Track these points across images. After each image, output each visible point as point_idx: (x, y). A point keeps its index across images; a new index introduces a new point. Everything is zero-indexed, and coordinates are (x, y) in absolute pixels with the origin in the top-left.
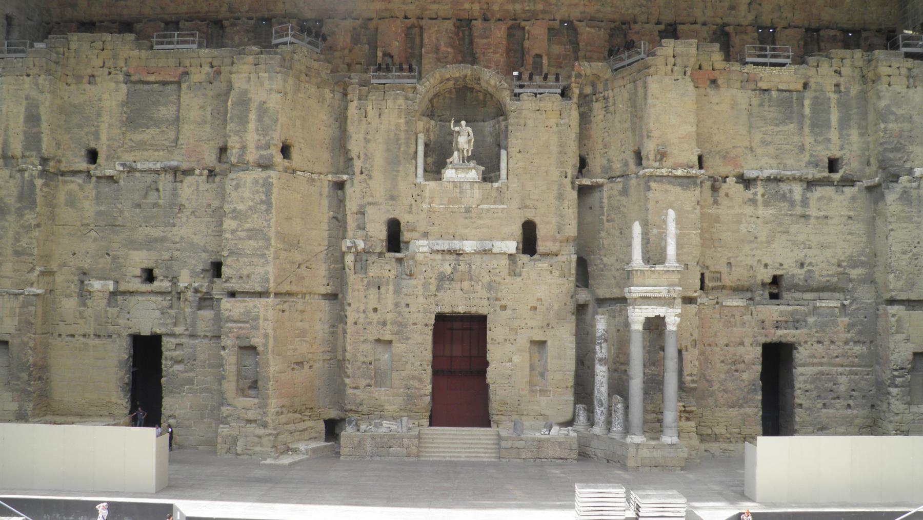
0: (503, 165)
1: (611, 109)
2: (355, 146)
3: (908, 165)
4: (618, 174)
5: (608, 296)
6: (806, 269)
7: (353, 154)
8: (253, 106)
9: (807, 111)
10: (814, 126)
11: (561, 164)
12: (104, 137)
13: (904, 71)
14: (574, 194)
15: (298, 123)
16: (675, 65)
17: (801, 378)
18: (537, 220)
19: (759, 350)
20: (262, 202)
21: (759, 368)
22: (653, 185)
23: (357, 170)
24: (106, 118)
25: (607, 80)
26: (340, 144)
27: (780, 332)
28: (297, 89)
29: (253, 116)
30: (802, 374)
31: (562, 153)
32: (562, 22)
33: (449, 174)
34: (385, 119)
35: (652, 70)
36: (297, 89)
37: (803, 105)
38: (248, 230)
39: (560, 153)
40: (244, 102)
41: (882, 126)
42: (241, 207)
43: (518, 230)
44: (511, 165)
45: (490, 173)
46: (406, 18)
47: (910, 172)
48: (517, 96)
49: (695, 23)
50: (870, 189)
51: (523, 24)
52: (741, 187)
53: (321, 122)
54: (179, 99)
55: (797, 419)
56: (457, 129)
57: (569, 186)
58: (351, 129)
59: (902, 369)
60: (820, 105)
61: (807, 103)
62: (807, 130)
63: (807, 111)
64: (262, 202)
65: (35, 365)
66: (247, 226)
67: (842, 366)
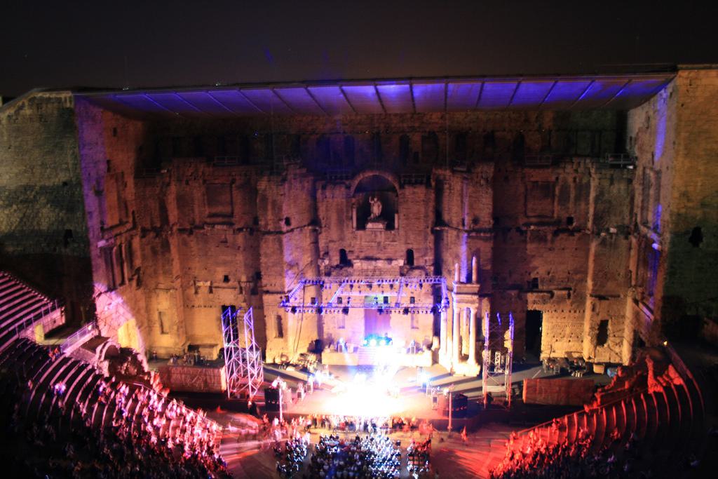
0: (396, 221)
1: (452, 191)
2: (322, 214)
3: (606, 226)
7: (321, 217)
8: (270, 200)
9: (557, 192)
10: (559, 201)
11: (426, 222)
12: (197, 211)
13: (608, 176)
14: (431, 238)
15: (292, 206)
20: (278, 249)
21: (524, 322)
23: (323, 225)
24: (196, 202)
26: (314, 209)
27: (535, 306)
28: (290, 189)
29: (270, 207)
31: (426, 216)
32: (429, 132)
33: (369, 225)
34: (334, 200)
36: (290, 189)
38: (272, 262)
39: (425, 217)
40: (264, 199)
42: (268, 252)
43: (404, 253)
44: (400, 222)
45: (390, 226)
46: (344, 132)
47: (608, 230)
49: (504, 130)
52: (518, 234)
53: (303, 198)
54: (231, 192)
56: (372, 202)
57: (430, 233)
58: (320, 205)
62: (556, 204)
64: (278, 249)
65: (179, 322)
66: (271, 261)
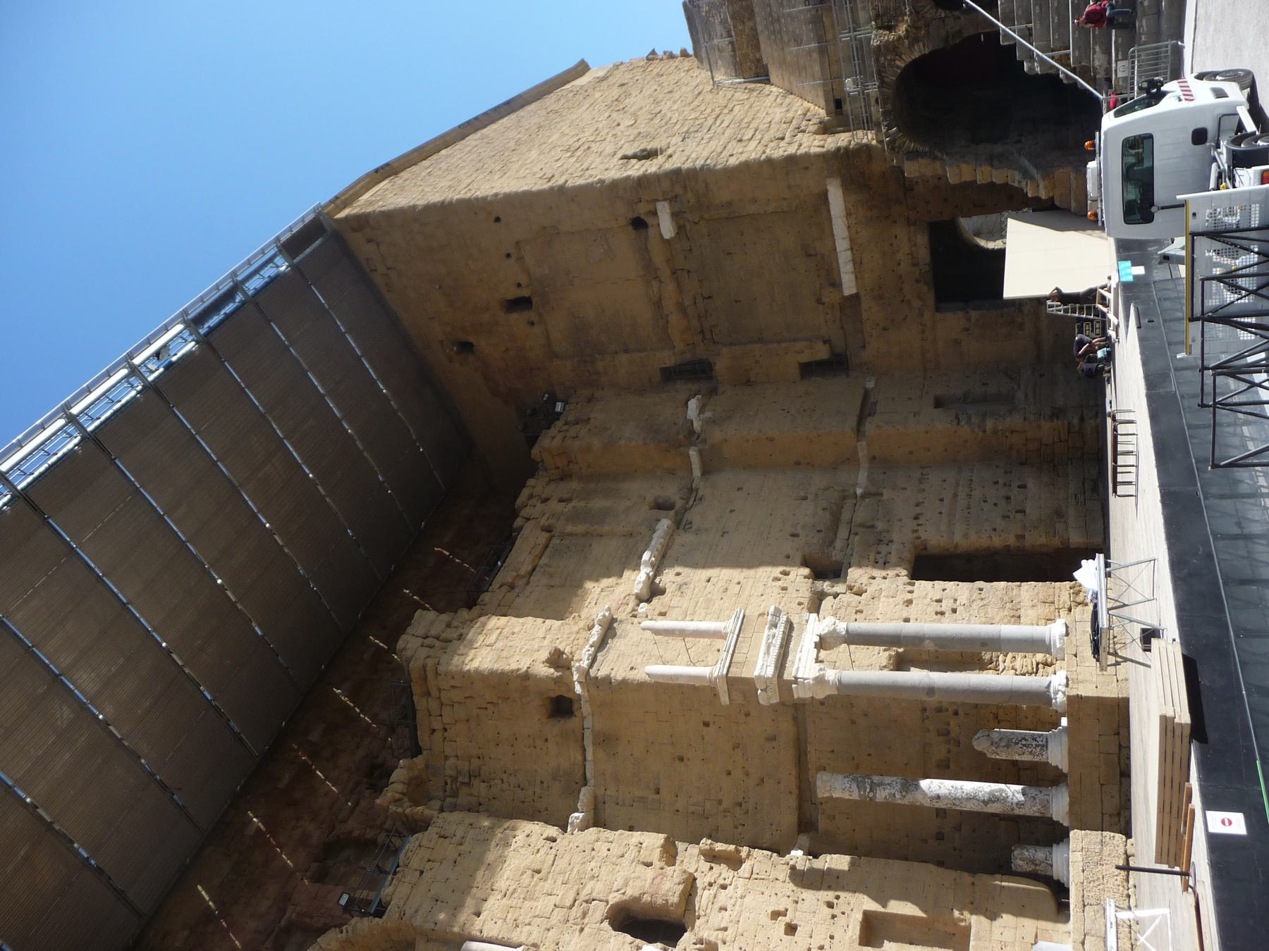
1: (475, 762)
4: (580, 758)
5: (793, 802)
6: (799, 531)
9: (580, 529)
16: (437, 638)
17: (973, 537)
18: (614, 898)
19: (917, 583)
22: (601, 674)
25: (427, 766)
30: (966, 536)
35: (430, 663)
37: (571, 534)
41: (623, 442)
48: (380, 913)
50: (706, 472)
51: (283, 923)
52: (655, 600)
55: (1043, 540)
59: (957, 418)
60: (575, 517)
61: (569, 528)
63: (580, 529)
67: (955, 495)
